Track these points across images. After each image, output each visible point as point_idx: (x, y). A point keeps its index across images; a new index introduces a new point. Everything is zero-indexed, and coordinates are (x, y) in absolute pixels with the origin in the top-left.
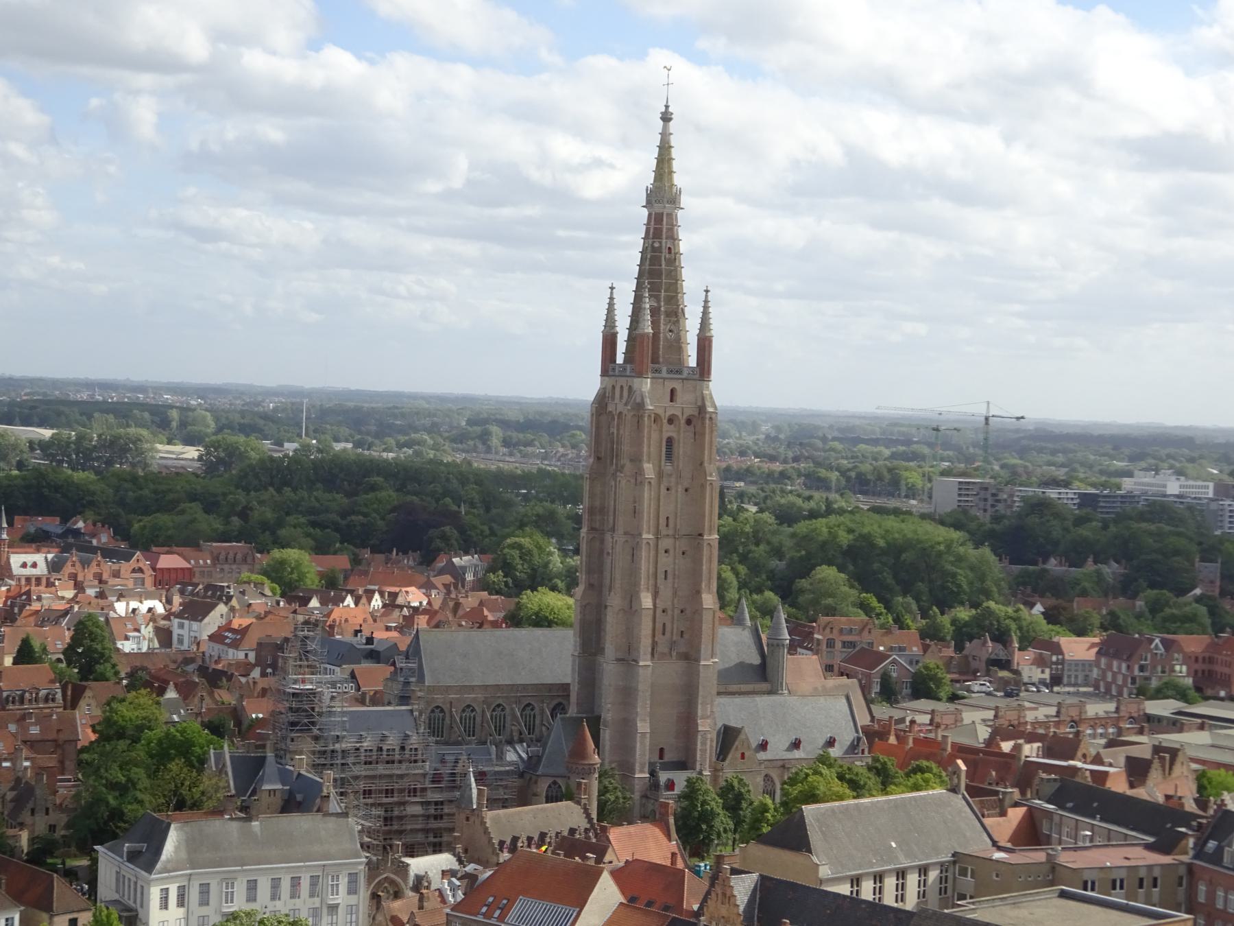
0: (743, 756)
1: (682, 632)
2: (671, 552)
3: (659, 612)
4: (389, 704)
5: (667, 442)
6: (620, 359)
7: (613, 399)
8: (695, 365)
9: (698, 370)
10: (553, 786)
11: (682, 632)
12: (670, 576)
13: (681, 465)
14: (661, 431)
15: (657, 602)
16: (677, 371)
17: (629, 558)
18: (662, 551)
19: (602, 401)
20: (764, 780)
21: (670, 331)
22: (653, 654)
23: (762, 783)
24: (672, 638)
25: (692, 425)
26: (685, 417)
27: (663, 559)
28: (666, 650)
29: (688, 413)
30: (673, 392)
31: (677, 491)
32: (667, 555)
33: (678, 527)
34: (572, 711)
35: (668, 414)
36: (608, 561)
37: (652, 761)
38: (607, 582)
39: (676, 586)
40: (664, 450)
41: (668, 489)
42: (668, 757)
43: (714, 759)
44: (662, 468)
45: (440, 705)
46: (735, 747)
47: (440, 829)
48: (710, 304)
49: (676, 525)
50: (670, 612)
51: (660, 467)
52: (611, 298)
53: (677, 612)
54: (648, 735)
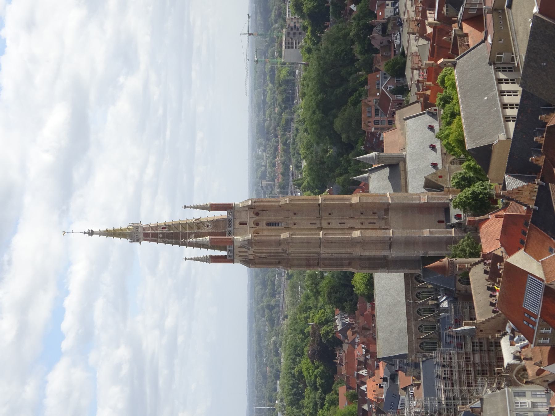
0: (440, 177)
1: (373, 213)
2: (330, 221)
3: (362, 227)
4: (419, 373)
6: (224, 253)
7: (246, 256)
8: (226, 212)
10: (461, 282)
11: (373, 213)
12: (343, 221)
13: (281, 217)
14: (263, 230)
15: (357, 228)
16: (230, 222)
17: (333, 244)
18: (329, 226)
19: (247, 262)
20: (453, 164)
21: (208, 226)
22: (386, 229)
23: (455, 165)
24: (377, 219)
25: (259, 212)
26: (254, 216)
27: (333, 226)
28: (384, 221)
29: (252, 215)
30: (241, 224)
31: (296, 219)
32: (331, 223)
33: (316, 218)
34: (419, 272)
36: (336, 255)
37: (445, 227)
38: (347, 256)
39: (348, 218)
40: (273, 227)
41: (295, 224)
42: (443, 218)
43: (443, 193)
44: (283, 228)
45: (419, 344)
46: (435, 181)
47: (487, 343)
49: (314, 219)
50: (363, 221)
51: (282, 229)
53: (362, 217)
54: (431, 230)
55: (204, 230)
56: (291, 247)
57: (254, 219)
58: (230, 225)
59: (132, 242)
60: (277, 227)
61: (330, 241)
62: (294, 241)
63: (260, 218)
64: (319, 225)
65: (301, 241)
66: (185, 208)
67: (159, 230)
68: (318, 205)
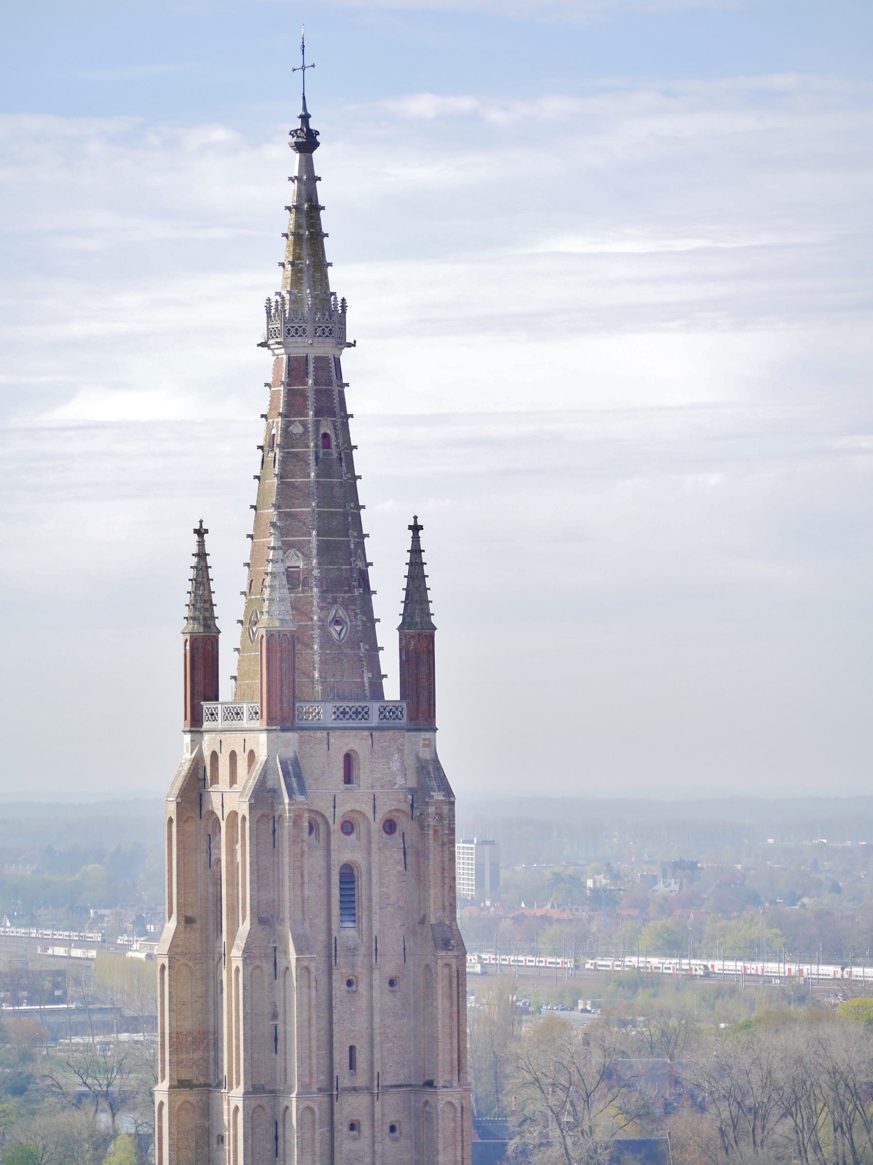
2: (365, 1129)
5: (342, 875)
7: (215, 780)
8: (398, 698)
9: (404, 705)
13: (376, 926)
14: (328, 851)
16: (357, 713)
18: (342, 1129)
21: (337, 622)
25: (397, 834)
26: (381, 815)
31: (371, 986)
33: (377, 1068)
35: (339, 812)
41: (349, 983)
44: (335, 934)
48: (425, 557)
49: (371, 1066)
52: (202, 555)
55: (322, 609)
56: (258, 967)
57: (370, 815)
58: (344, 713)
59: (268, 313)
60: (336, 911)
61: (280, 1130)
62: (280, 981)
63: (375, 837)
64: (345, 1083)
65: (280, 1010)
66: (410, 527)
67: (317, 424)
68: (427, 1078)
